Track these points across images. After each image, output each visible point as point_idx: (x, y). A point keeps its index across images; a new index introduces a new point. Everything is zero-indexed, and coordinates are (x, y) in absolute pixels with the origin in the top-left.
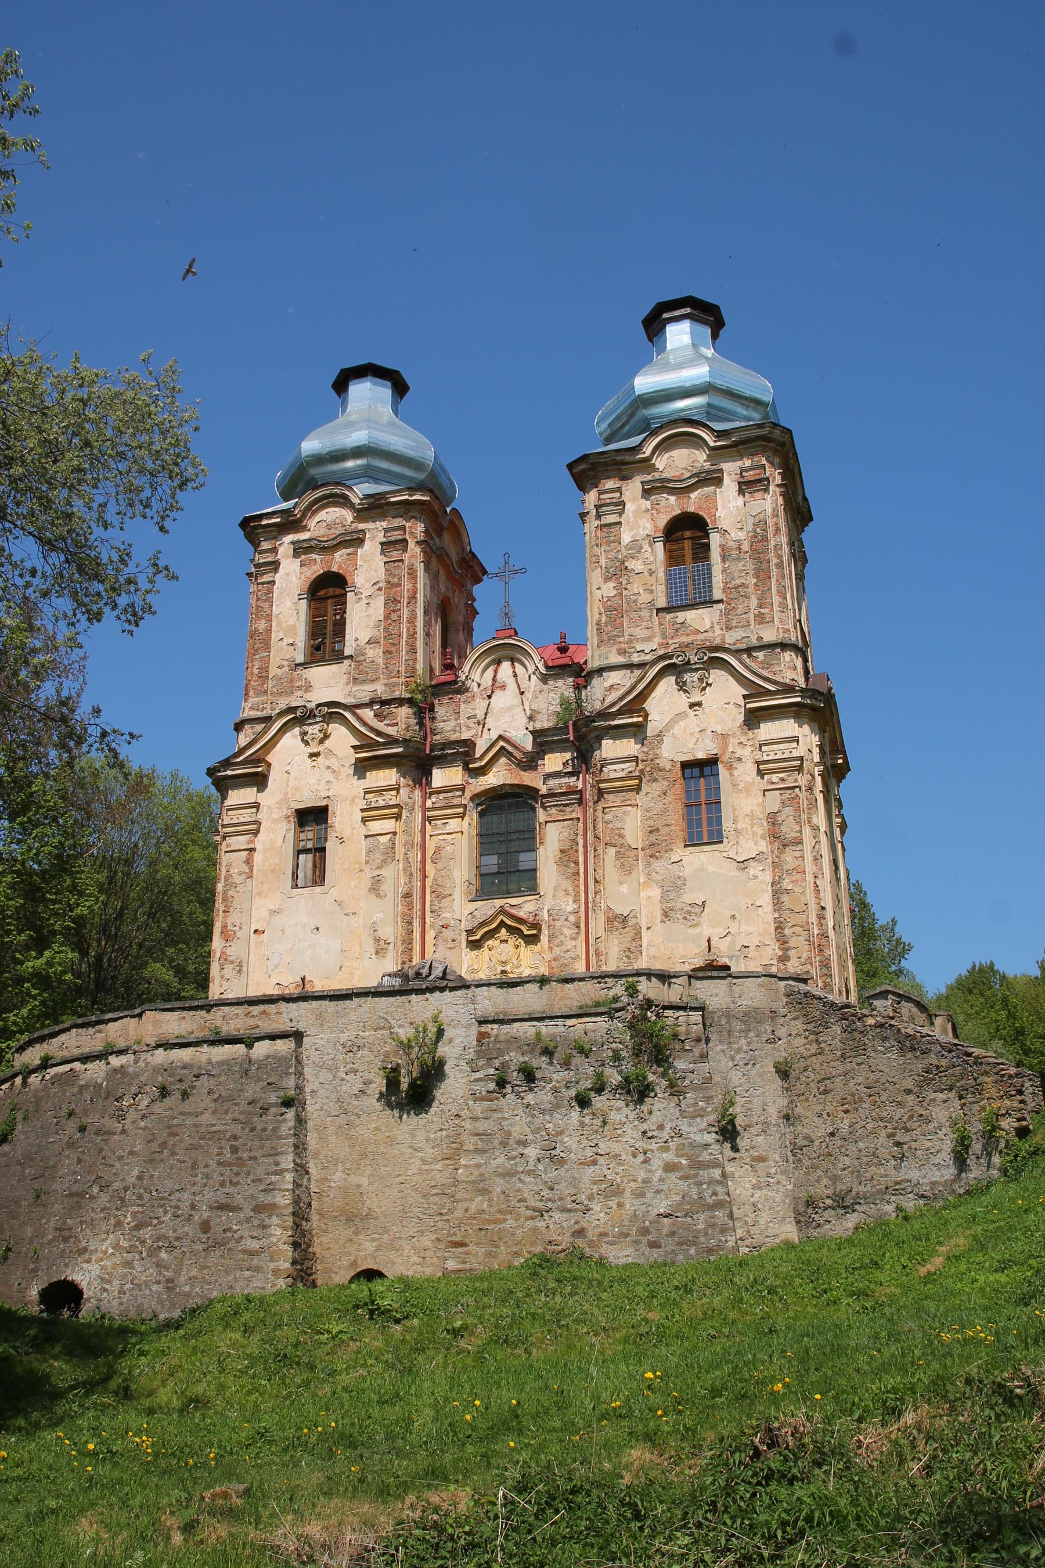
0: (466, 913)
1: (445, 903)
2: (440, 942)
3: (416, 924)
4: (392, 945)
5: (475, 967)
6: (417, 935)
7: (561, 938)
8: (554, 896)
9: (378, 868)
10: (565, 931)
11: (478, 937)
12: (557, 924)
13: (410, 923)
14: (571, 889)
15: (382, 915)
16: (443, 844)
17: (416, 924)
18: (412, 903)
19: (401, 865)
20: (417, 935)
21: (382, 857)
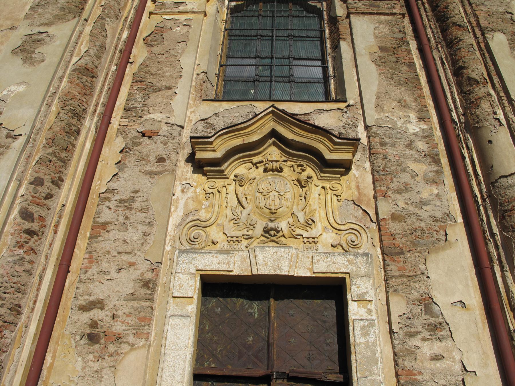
0: (195, 118)
1: (154, 98)
2: (131, 160)
3: (90, 124)
4: (21, 140)
5: (203, 215)
6: (85, 143)
7: (406, 177)
8: (379, 107)
9: (48, 24)
10: (412, 166)
11: (218, 154)
12: (390, 151)
13: (78, 115)
14: (409, 99)
15: (21, 89)
16: (169, 24)
17: (90, 124)
18: (92, 87)
19: (88, 29)
20: (85, 143)
21: (56, 12)
